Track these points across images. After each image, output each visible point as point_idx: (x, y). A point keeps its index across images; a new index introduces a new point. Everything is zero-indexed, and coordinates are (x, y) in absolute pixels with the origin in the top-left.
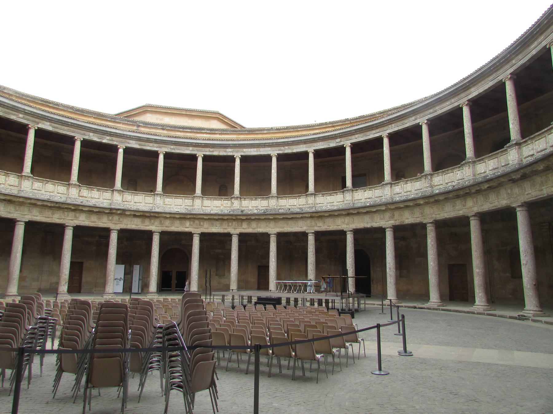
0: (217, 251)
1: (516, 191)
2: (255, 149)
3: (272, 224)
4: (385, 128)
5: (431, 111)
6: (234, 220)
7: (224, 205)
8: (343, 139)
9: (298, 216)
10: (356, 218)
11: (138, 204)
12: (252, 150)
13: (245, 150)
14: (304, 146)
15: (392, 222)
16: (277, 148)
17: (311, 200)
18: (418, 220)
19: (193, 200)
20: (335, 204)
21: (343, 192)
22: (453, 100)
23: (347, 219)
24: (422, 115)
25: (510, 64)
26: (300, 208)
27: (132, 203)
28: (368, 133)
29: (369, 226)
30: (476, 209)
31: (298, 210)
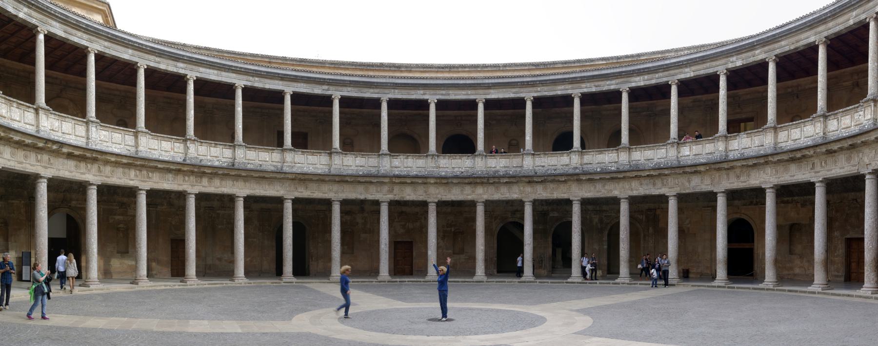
0: (117, 217)
1: (528, 189)
2: (216, 72)
3: (240, 184)
4: (386, 91)
5: (444, 92)
6: (192, 172)
7: (176, 150)
8: (331, 88)
9: (278, 176)
10: (347, 187)
11: (67, 136)
12: (211, 71)
13: (202, 69)
14: (281, 82)
15: (390, 197)
16: (245, 77)
17: (289, 157)
18: (421, 198)
19: (136, 137)
20: (318, 166)
21: (330, 154)
22: (469, 92)
23: (336, 187)
24: (432, 92)
25: (535, 89)
26: (274, 166)
27: (60, 134)
28: (365, 90)
29: (362, 197)
30: (486, 197)
31: (273, 168)
